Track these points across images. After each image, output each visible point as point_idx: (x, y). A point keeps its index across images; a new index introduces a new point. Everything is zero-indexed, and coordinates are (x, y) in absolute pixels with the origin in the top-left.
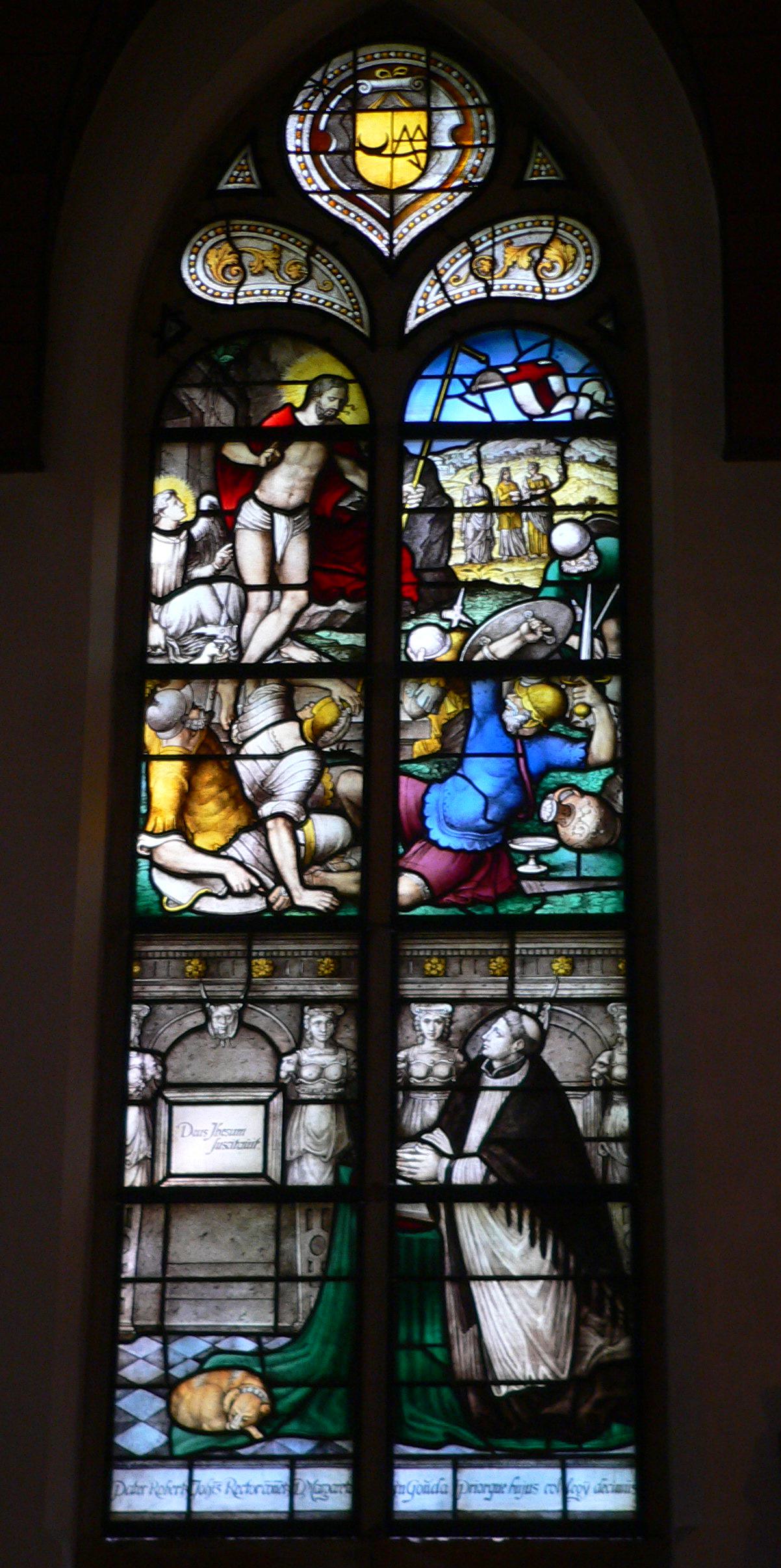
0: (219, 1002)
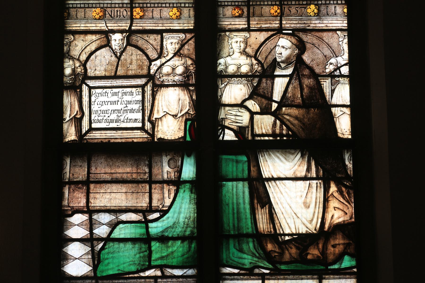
0: (113, 32)
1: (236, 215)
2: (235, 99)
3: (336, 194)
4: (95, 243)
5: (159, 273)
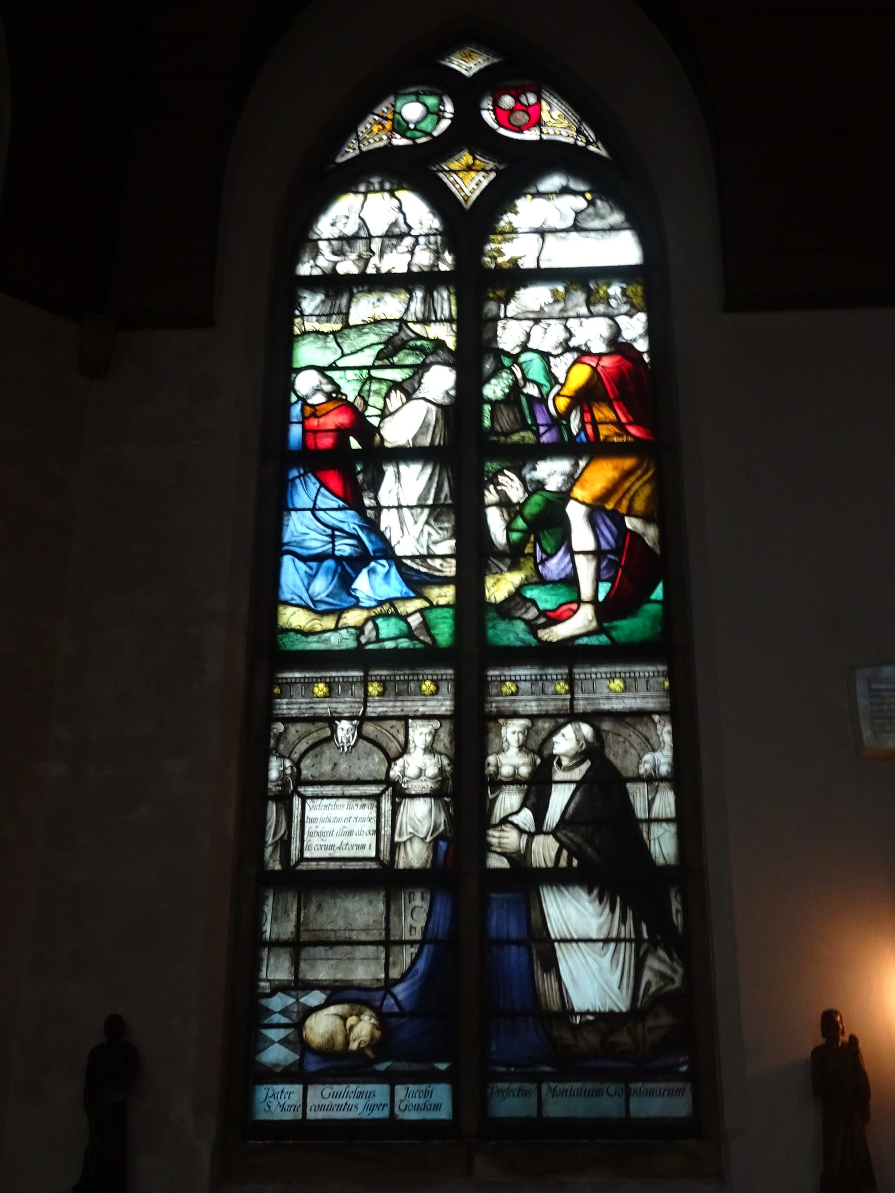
0: (340, 719)
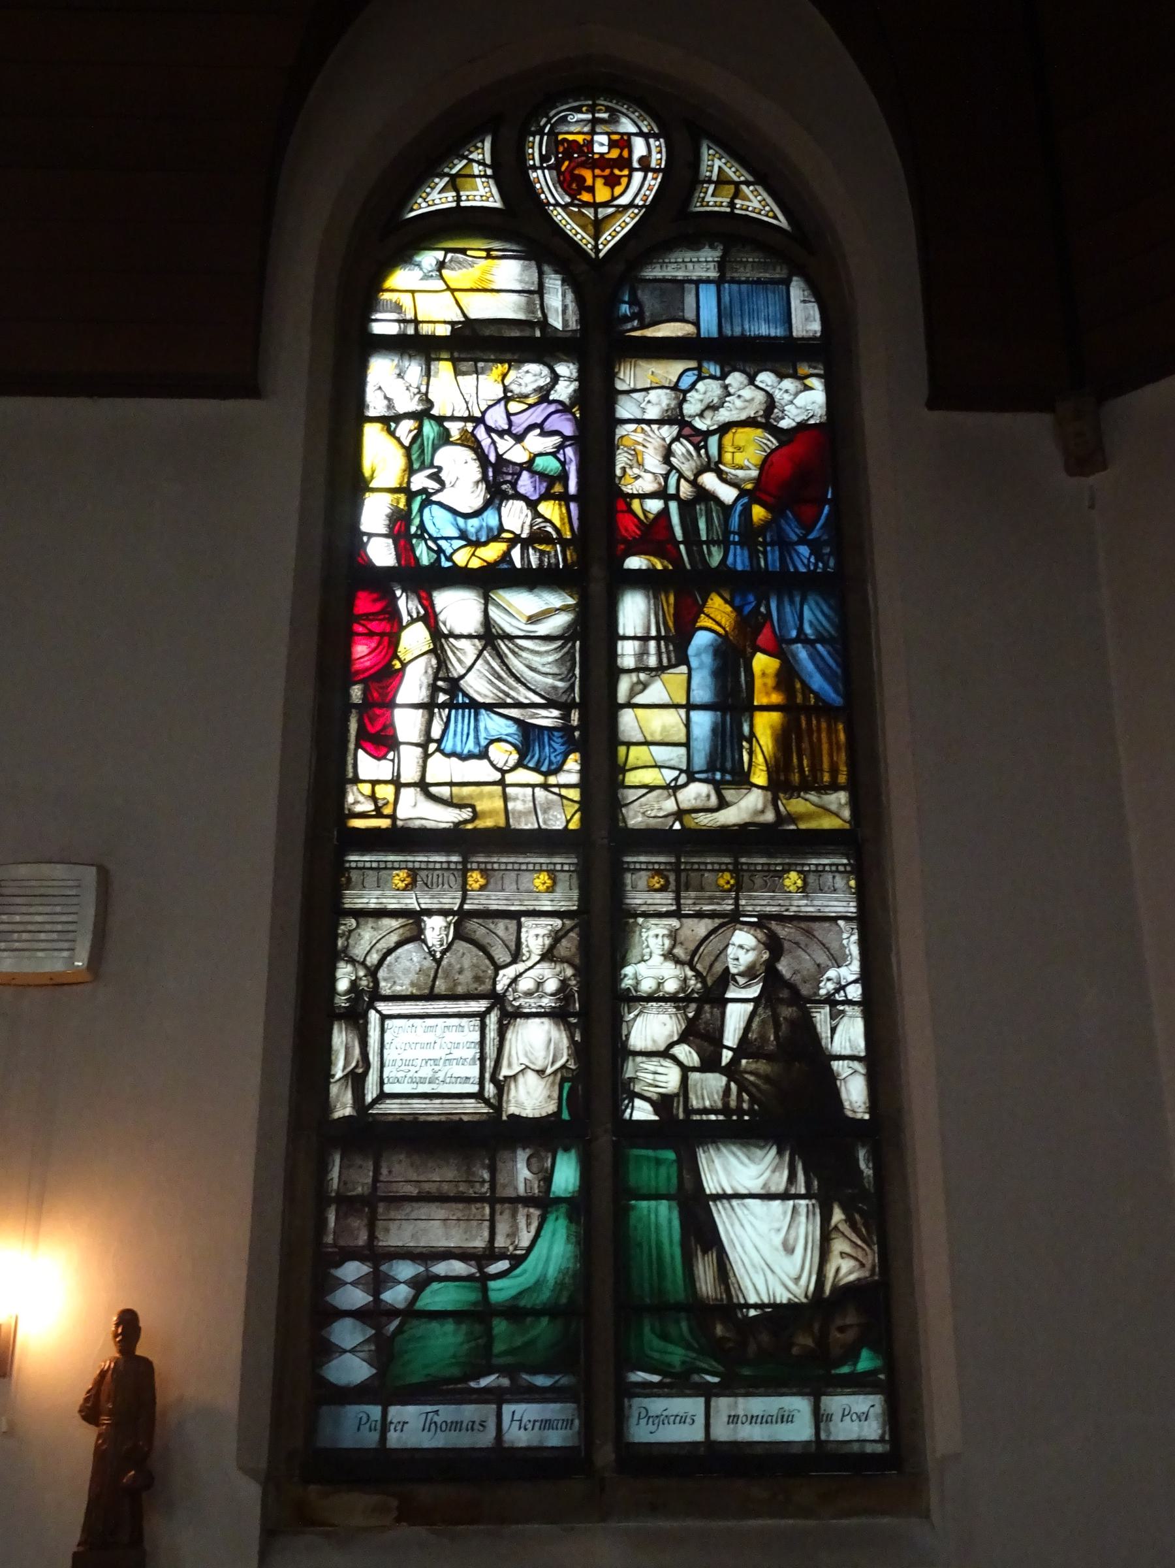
0: (429, 913)
1: (655, 1266)
2: (654, 1041)
3: (844, 1228)
4: (384, 1319)
5: (505, 1382)
